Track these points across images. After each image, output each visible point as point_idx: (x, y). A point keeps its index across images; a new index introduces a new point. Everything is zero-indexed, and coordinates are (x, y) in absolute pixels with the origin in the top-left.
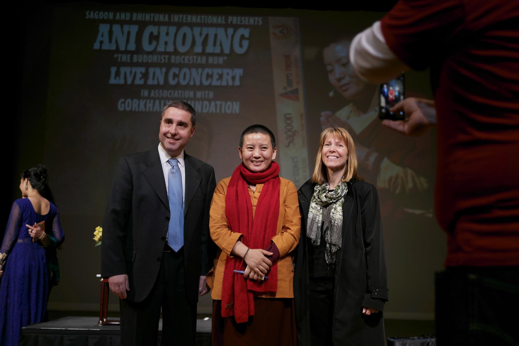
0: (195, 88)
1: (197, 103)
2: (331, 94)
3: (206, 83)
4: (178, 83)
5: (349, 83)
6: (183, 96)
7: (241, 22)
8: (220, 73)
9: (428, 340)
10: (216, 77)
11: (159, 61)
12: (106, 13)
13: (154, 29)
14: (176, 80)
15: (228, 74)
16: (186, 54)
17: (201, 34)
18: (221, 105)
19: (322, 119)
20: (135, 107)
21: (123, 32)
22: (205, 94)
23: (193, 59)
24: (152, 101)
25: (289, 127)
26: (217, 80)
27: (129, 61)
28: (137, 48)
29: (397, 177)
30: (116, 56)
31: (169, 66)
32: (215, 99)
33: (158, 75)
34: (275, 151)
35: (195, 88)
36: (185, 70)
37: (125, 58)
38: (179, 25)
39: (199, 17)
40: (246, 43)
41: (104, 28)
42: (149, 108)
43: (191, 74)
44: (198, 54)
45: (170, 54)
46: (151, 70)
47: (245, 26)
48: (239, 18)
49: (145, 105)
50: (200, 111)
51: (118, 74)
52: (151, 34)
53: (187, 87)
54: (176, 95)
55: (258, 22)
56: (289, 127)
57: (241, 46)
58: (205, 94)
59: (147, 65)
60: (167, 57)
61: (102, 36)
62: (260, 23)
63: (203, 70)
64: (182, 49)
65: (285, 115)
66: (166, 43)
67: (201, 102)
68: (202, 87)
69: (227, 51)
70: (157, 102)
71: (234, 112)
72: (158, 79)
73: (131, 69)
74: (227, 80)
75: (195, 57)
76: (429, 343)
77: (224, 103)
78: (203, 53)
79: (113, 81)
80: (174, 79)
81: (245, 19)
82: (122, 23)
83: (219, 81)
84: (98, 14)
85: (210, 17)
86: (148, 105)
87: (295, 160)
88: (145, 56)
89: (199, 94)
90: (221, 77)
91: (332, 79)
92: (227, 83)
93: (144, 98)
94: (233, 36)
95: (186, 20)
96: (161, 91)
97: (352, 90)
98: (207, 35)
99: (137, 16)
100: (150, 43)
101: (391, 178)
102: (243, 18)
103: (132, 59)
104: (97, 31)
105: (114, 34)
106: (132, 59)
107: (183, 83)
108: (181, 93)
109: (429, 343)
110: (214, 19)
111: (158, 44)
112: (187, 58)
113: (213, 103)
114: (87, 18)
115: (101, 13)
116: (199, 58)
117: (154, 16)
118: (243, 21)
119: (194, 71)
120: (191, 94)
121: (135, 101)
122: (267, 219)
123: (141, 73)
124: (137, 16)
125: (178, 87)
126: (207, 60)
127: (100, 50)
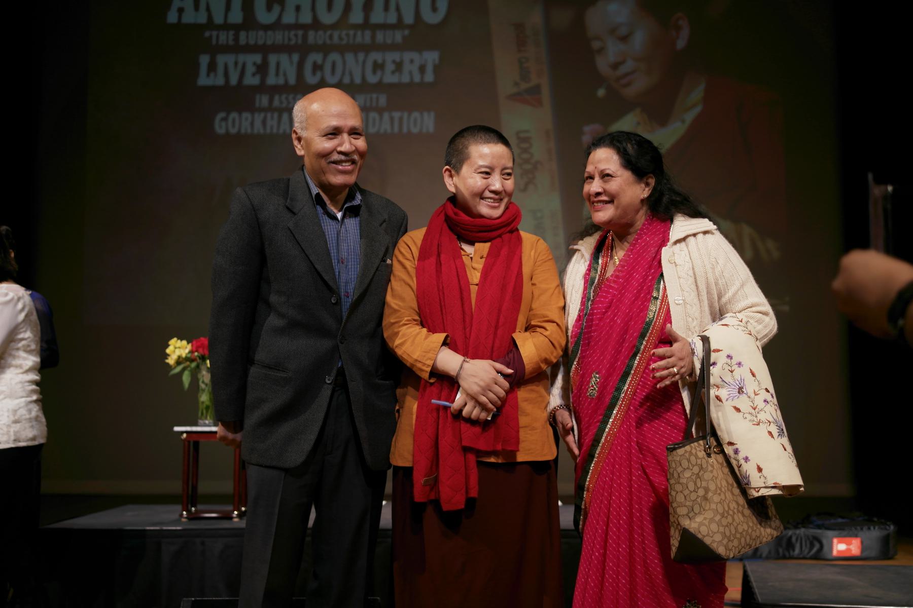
2: (601, 92)
3: (372, 79)
8: (398, 60)
9: (790, 533)
10: (390, 67)
14: (319, 74)
15: (412, 61)
16: (334, 27)
18: (401, 119)
20: (246, 127)
22: (371, 99)
23: (347, 35)
24: (276, 115)
25: (525, 156)
26: (393, 72)
27: (231, 42)
28: (245, 18)
30: (207, 34)
31: (304, 49)
36: (334, 56)
37: (225, 38)
42: (272, 128)
43: (344, 63)
44: (356, 27)
45: (305, 27)
46: (273, 59)
49: (264, 123)
51: (212, 67)
56: (525, 156)
58: (371, 99)
59: (265, 50)
60: (300, 33)
63: (366, 56)
64: (327, 19)
65: (518, 133)
66: (298, 8)
69: (409, 19)
71: (424, 130)
72: (285, 75)
74: (411, 73)
75: (352, 32)
76: (791, 537)
77: (406, 115)
78: (366, 25)
79: (204, 80)
83: (397, 74)
86: (269, 123)
88: (261, 33)
90: (399, 67)
91: (602, 64)
92: (412, 78)
93: (261, 110)
97: (640, 84)
100: (269, 8)
103: (236, 38)
106: (236, 38)
109: (791, 537)
111: (282, 10)
112: (336, 35)
113: (386, 116)
116: (359, 33)
119: (350, 57)
121: (246, 115)
123: (255, 64)
126: (373, 37)
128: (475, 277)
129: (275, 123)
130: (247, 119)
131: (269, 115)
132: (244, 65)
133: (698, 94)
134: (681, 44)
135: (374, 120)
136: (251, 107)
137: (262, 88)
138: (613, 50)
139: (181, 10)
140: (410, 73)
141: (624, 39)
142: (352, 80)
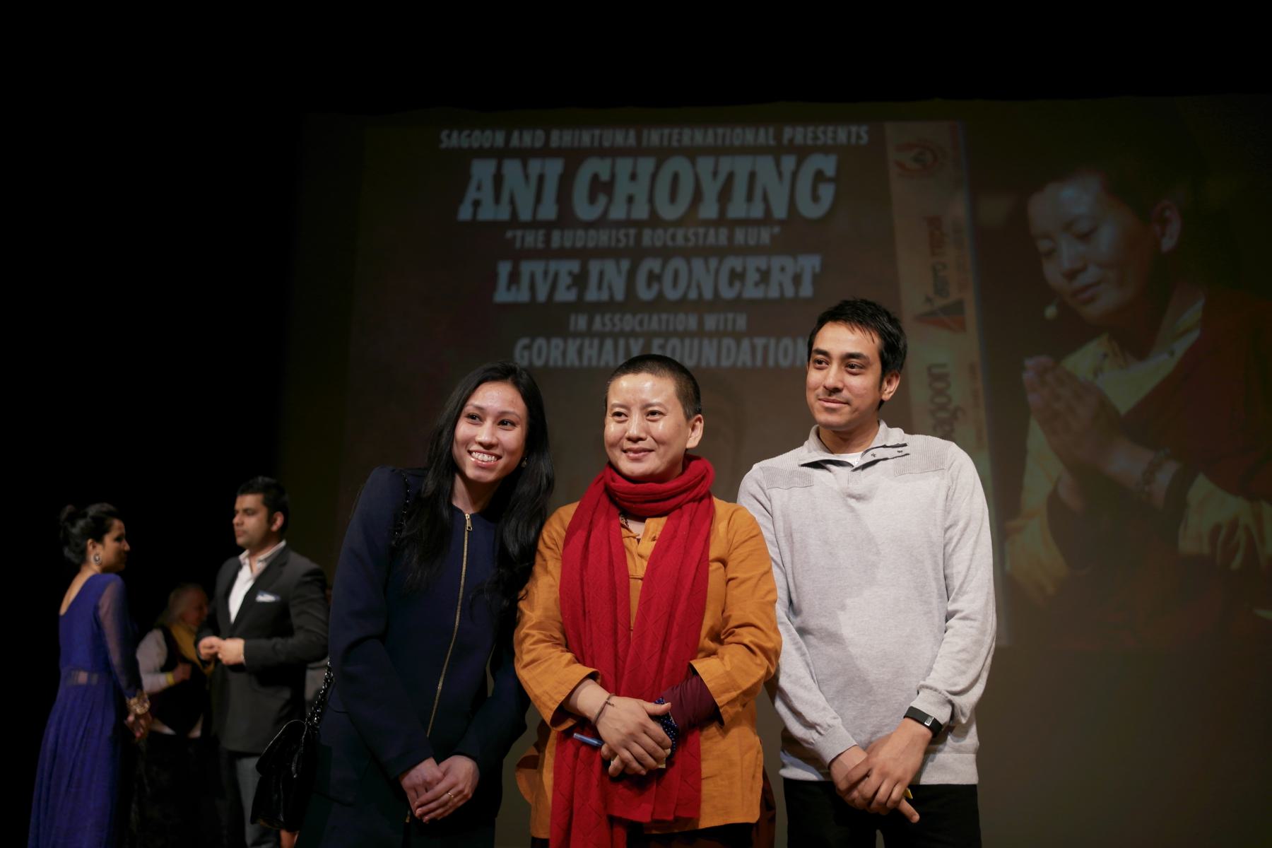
1: (706, 342)
2: (1051, 312)
3: (728, 293)
4: (660, 295)
6: (671, 328)
7: (816, 138)
8: (764, 266)
10: (752, 276)
11: (613, 244)
12: (488, 133)
13: (601, 167)
14: (655, 287)
15: (783, 269)
16: (679, 223)
17: (715, 174)
18: (766, 348)
19: (1028, 376)
21: (527, 177)
22: (726, 320)
23: (696, 235)
24: (596, 342)
26: (757, 284)
27: (540, 245)
29: (1234, 525)
31: (637, 254)
32: (751, 332)
33: (610, 278)
34: (700, 426)
35: (700, 306)
36: (678, 263)
37: (532, 239)
38: (662, 154)
39: (710, 132)
40: (827, 192)
41: (482, 170)
42: (590, 359)
43: (690, 271)
44: (707, 223)
45: (639, 225)
46: (594, 267)
47: (825, 150)
48: (810, 129)
49: (580, 352)
50: (713, 363)
51: (514, 278)
52: (595, 177)
53: (682, 305)
54: (654, 325)
55: (859, 137)
57: (815, 198)
58: (726, 320)
59: (584, 255)
60: (632, 232)
61: (479, 188)
62: (865, 139)
63: (720, 262)
64: (669, 212)
65: (929, 369)
66: (630, 199)
67: (715, 342)
68: (718, 305)
69: (780, 212)
70: (609, 344)
72: (610, 288)
74: (781, 285)
75: (701, 231)
77: (772, 342)
78: (722, 221)
79: (503, 295)
81: (825, 133)
82: (524, 155)
83: (762, 287)
84: (469, 136)
85: (738, 131)
86: (587, 352)
88: (580, 233)
89: (711, 322)
90: (765, 276)
91: (1053, 273)
93: (577, 335)
94: (795, 175)
95: (679, 141)
96: (617, 317)
97: (1108, 299)
98: (731, 176)
99: (561, 138)
100: (592, 199)
101: (1217, 529)
102: (821, 129)
103: (548, 240)
104: (466, 177)
105: (505, 180)
106: (548, 240)
107: (672, 295)
108: (668, 321)
110: (748, 136)
111: (610, 201)
112: (680, 234)
113: (746, 343)
114: (443, 146)
115: (477, 133)
116: (712, 232)
117: (601, 137)
118: (820, 135)
119: (698, 264)
120: (692, 322)
121: (557, 342)
122: (671, 616)
123: (570, 273)
124: (561, 138)
125: (659, 304)
126: (731, 237)
127: (474, 224)
128: (638, 568)
129: (594, 352)
130: (557, 347)
131: (587, 342)
132: (556, 275)
133: (1193, 314)
134: (1168, 244)
135: (729, 350)
136: (562, 331)
137: (579, 306)
138: (1068, 252)
139: (477, 204)
140: (780, 286)
141: (1085, 237)
142: (700, 295)
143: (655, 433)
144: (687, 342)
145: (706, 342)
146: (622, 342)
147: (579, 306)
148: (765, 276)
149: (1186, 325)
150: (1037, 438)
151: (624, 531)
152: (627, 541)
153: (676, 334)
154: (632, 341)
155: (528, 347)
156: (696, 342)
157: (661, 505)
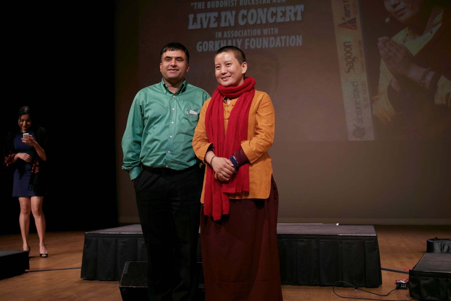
0: (262, 26)
1: (264, 39)
2: (387, 20)
3: (271, 21)
4: (247, 22)
5: (404, 8)
6: (251, 35)
8: (284, 10)
10: (280, 14)
11: (229, 5)
14: (245, 20)
15: (290, 11)
18: (285, 40)
19: (380, 44)
22: (271, 30)
24: (225, 41)
25: (348, 55)
26: (281, 17)
27: (203, 8)
30: (192, 4)
31: (238, 8)
33: (229, 18)
35: (262, 26)
36: (253, 11)
46: (223, 14)
50: (267, 46)
51: (195, 20)
53: (255, 26)
54: (246, 34)
56: (348, 55)
58: (271, 30)
59: (219, 10)
65: (344, 43)
67: (267, 38)
68: (267, 25)
71: (297, 45)
73: (206, 15)
74: (290, 16)
77: (288, 37)
79: (191, 26)
80: (243, 20)
83: (283, 18)
87: (356, 84)
89: (265, 32)
90: (284, 14)
96: (232, 32)
97: (408, 14)
107: (251, 23)
113: (278, 38)
119: (260, 10)
120: (259, 32)
121: (210, 42)
123: (215, 17)
125: (247, 26)
131: (222, 41)
133: (439, 17)
135: (272, 40)
137: (219, 29)
140: (290, 17)
143: (229, 71)
144: (257, 39)
145: (264, 39)
146: (234, 41)
147: (219, 29)
148: (284, 14)
149: (437, 21)
150: (383, 66)
151: (224, 103)
152: (225, 108)
153: (253, 37)
154: (238, 40)
155: (201, 45)
156: (261, 39)
157: (235, 93)
